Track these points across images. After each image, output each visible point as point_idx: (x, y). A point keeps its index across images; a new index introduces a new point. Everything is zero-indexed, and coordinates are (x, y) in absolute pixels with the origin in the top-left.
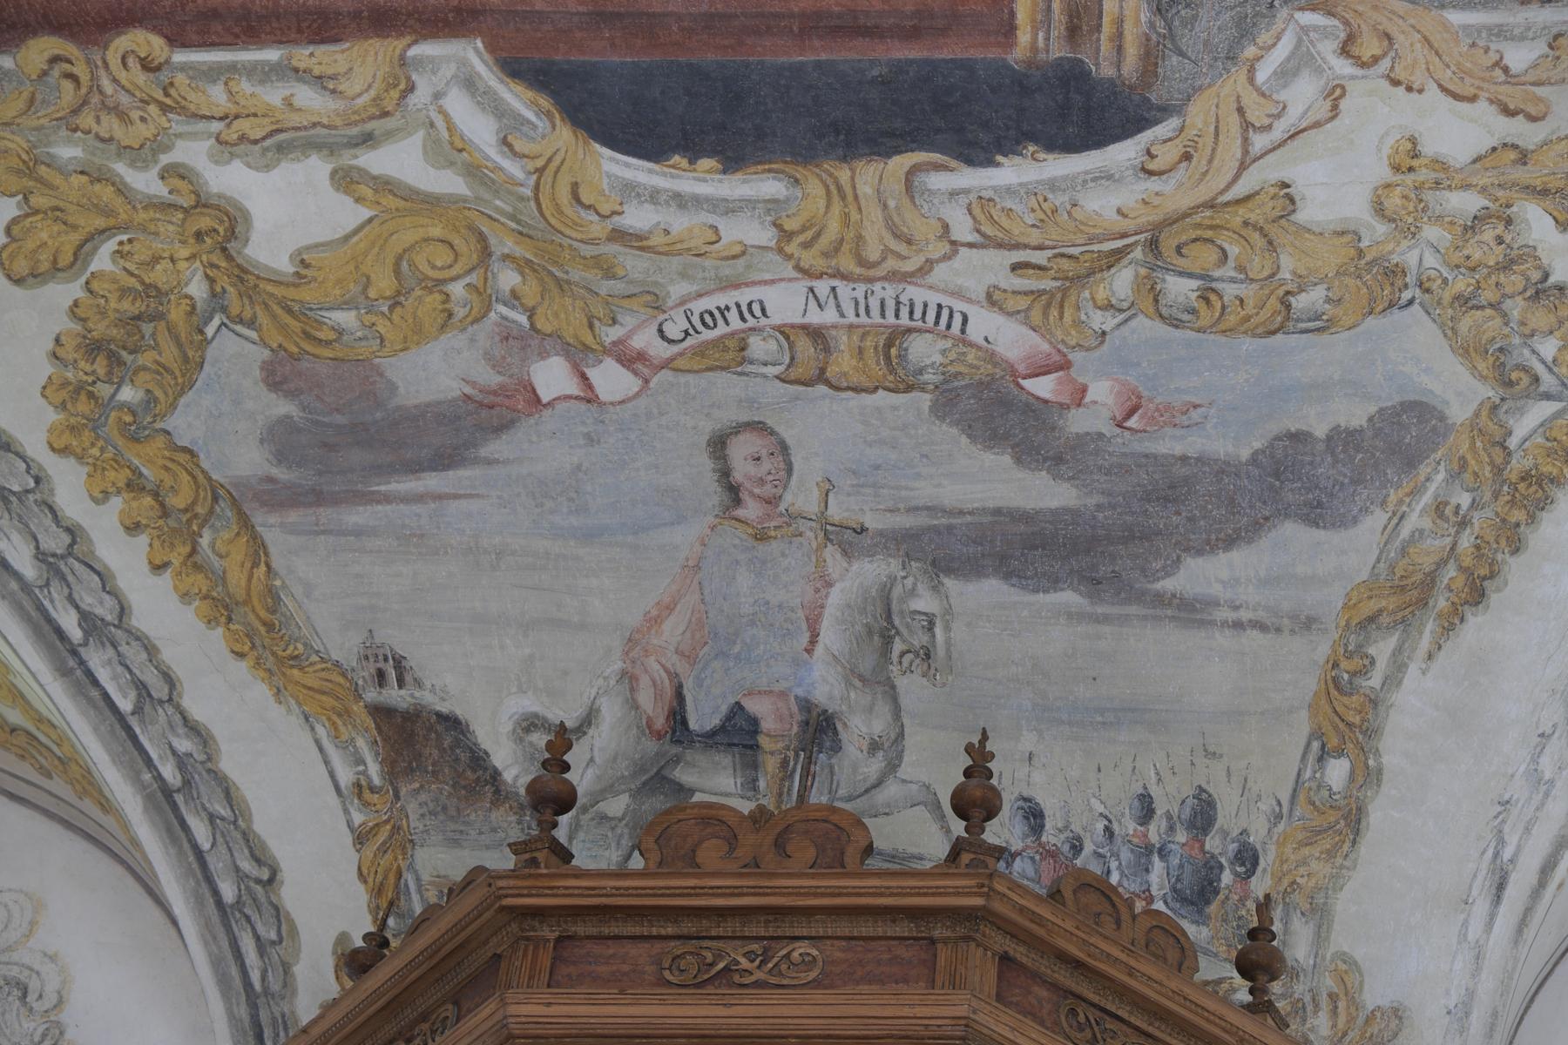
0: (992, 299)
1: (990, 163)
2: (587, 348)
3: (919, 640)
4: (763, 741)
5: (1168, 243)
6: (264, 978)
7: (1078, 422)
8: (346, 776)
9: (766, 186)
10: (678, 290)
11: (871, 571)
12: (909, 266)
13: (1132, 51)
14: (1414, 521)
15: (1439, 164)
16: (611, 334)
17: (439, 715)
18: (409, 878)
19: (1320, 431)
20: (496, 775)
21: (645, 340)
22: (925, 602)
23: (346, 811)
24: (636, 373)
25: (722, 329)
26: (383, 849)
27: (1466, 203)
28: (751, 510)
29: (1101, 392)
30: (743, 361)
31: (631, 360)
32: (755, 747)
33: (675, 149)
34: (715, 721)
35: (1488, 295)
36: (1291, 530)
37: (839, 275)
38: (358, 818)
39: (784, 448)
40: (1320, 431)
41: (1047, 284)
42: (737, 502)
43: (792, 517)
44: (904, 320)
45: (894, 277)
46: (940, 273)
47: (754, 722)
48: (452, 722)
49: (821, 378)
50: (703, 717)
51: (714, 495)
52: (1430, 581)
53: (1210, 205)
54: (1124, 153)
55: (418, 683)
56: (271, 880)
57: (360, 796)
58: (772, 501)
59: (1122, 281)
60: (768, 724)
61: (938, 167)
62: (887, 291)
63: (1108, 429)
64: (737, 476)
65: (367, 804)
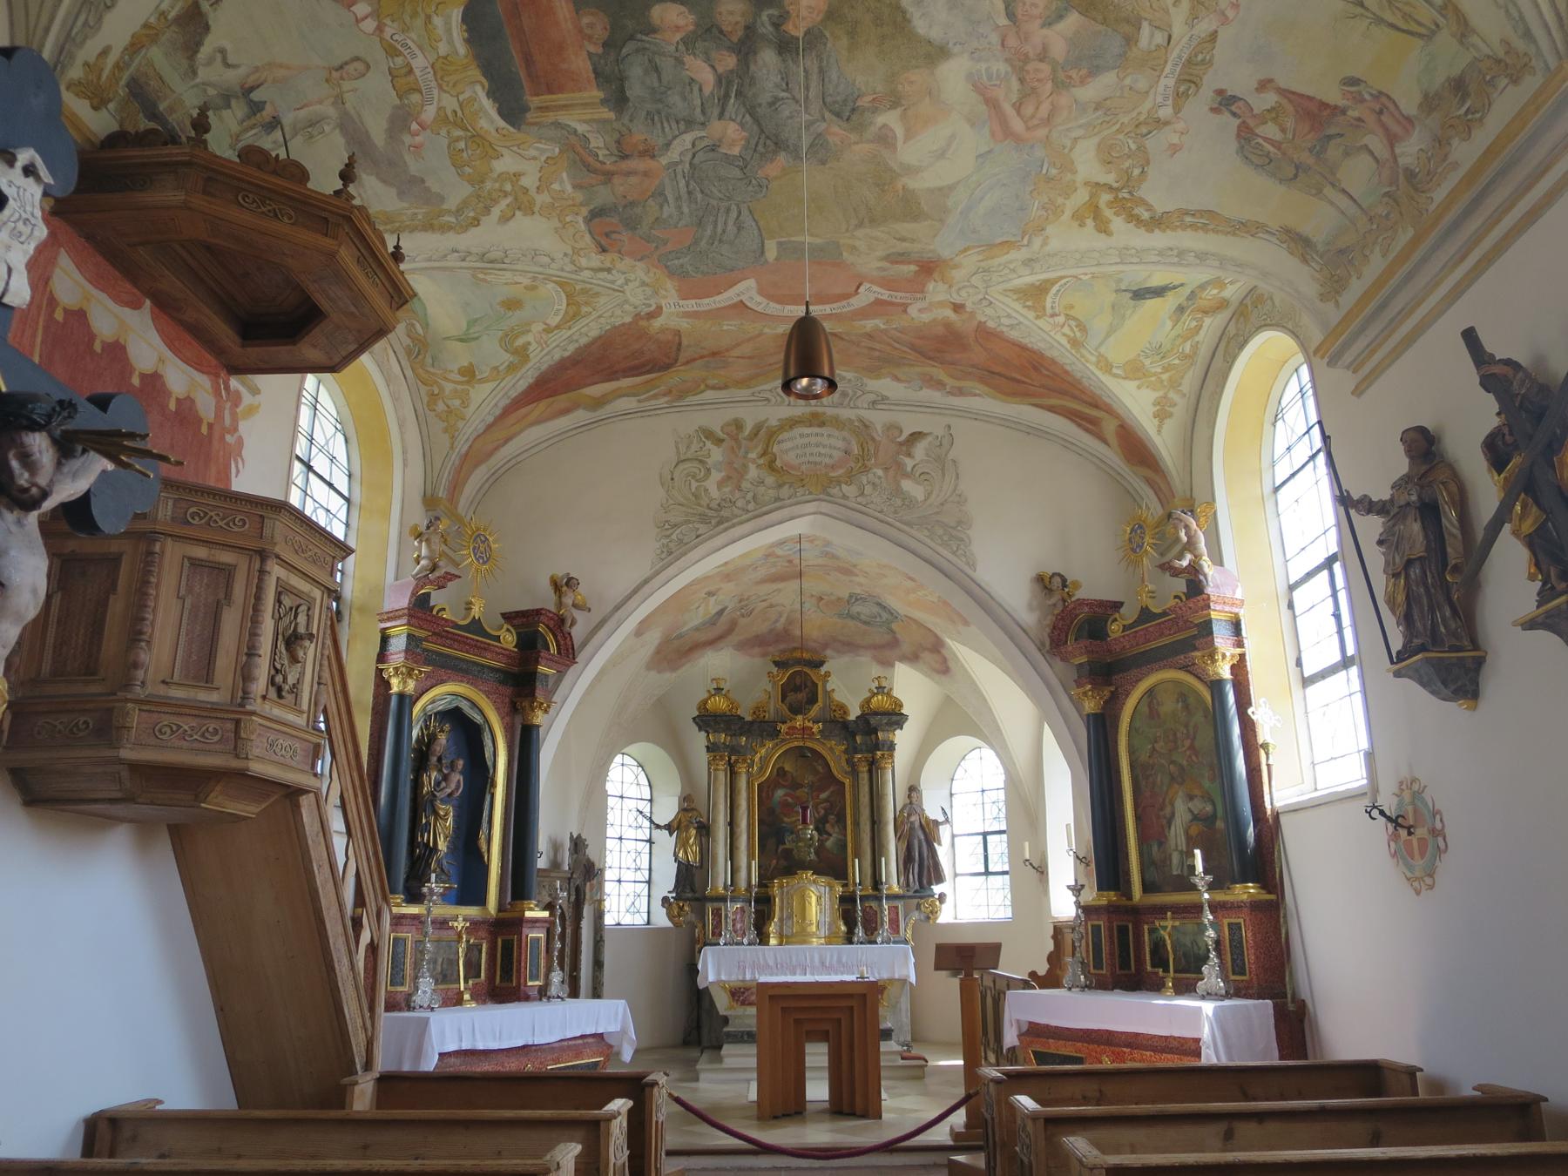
0: (440, 109)
1: (489, 98)
2: (379, 17)
3: (315, 133)
4: (259, 115)
5: (475, 139)
6: (77, 34)
7: (407, 139)
8: (164, 6)
9: (462, 49)
10: (413, 35)
11: (332, 112)
12: (445, 88)
13: (538, 120)
14: (409, 212)
15: (517, 181)
16: (388, 21)
17: (207, 22)
18: (144, 51)
19: (427, 185)
20: (197, 52)
21: (388, 32)
22: (327, 128)
23: (152, 15)
24: (375, 31)
25: (402, 50)
26: (147, 36)
27: (508, 187)
28: (335, 74)
29: (418, 139)
30: (392, 57)
31: (380, 29)
32: (255, 114)
33: (467, 25)
34: (256, 99)
35: (482, 200)
36: (394, 191)
37: (435, 73)
38: (152, 20)
39: (364, 75)
40: (427, 185)
41: (451, 119)
42: (337, 70)
43: (339, 86)
44: (424, 91)
45: (440, 87)
46: (445, 95)
47: (263, 109)
48: (207, 28)
49: (393, 77)
50: (255, 96)
51: (337, 63)
52: (393, 222)
53: (490, 144)
54: (502, 123)
55: (216, 9)
56: (108, 7)
57: (160, 15)
58: (342, 78)
59: (458, 133)
60: (264, 113)
61: (483, 87)
62: (434, 84)
63: (407, 145)
64: (346, 67)
65: (159, 19)
